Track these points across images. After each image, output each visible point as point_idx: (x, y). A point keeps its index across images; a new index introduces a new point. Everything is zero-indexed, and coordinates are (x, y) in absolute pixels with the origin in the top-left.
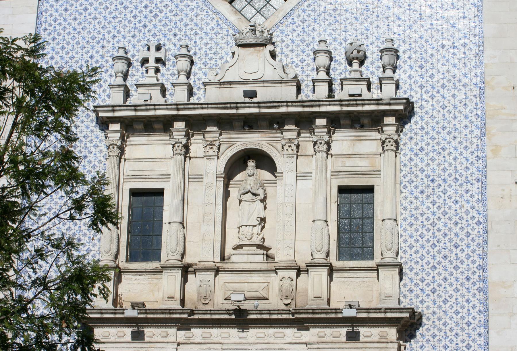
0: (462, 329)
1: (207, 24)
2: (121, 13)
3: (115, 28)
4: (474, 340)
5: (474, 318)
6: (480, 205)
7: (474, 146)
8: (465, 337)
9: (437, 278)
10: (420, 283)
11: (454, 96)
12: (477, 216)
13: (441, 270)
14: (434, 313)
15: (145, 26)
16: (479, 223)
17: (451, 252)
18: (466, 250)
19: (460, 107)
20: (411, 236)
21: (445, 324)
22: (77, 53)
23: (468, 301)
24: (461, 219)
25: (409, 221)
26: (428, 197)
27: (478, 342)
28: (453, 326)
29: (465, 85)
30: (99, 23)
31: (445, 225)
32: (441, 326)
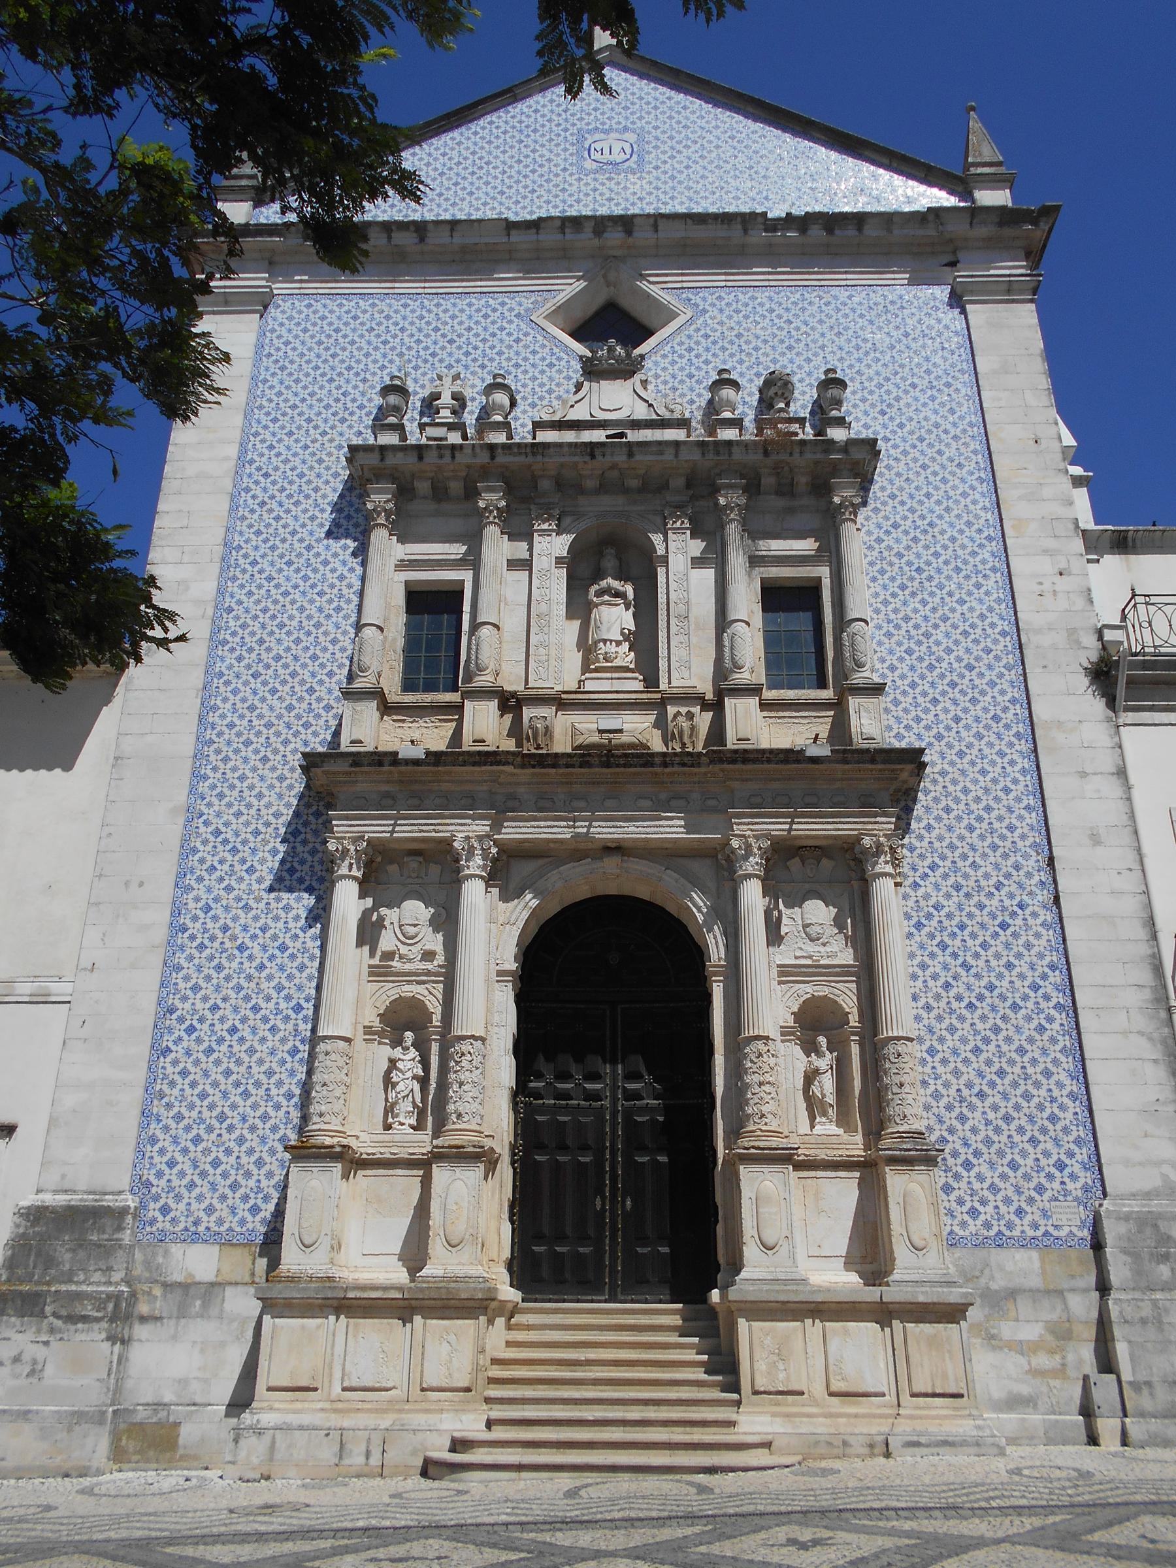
0: (996, 798)
1: (534, 352)
2: (395, 336)
3: (384, 356)
4: (1021, 818)
5: (1015, 781)
6: (1003, 606)
7: (982, 521)
8: (1003, 812)
9: (942, 717)
10: (914, 725)
11: (940, 453)
12: (1000, 623)
13: (948, 704)
14: (943, 773)
15: (434, 355)
16: (1004, 634)
17: (962, 677)
18: (987, 673)
19: (951, 467)
20: (891, 652)
21: (965, 791)
22: (321, 388)
23: (1001, 754)
24: (973, 626)
25: (884, 630)
26: (913, 594)
27: (1028, 821)
28: (980, 793)
29: (955, 437)
30: (360, 349)
31: (947, 635)
32: (959, 794)
